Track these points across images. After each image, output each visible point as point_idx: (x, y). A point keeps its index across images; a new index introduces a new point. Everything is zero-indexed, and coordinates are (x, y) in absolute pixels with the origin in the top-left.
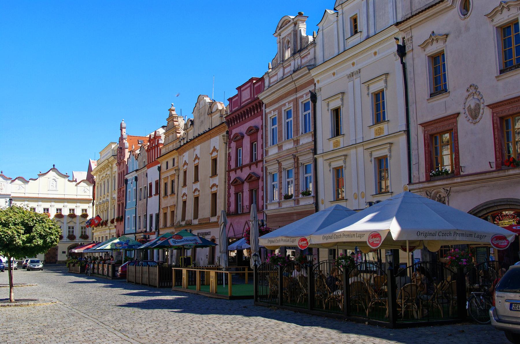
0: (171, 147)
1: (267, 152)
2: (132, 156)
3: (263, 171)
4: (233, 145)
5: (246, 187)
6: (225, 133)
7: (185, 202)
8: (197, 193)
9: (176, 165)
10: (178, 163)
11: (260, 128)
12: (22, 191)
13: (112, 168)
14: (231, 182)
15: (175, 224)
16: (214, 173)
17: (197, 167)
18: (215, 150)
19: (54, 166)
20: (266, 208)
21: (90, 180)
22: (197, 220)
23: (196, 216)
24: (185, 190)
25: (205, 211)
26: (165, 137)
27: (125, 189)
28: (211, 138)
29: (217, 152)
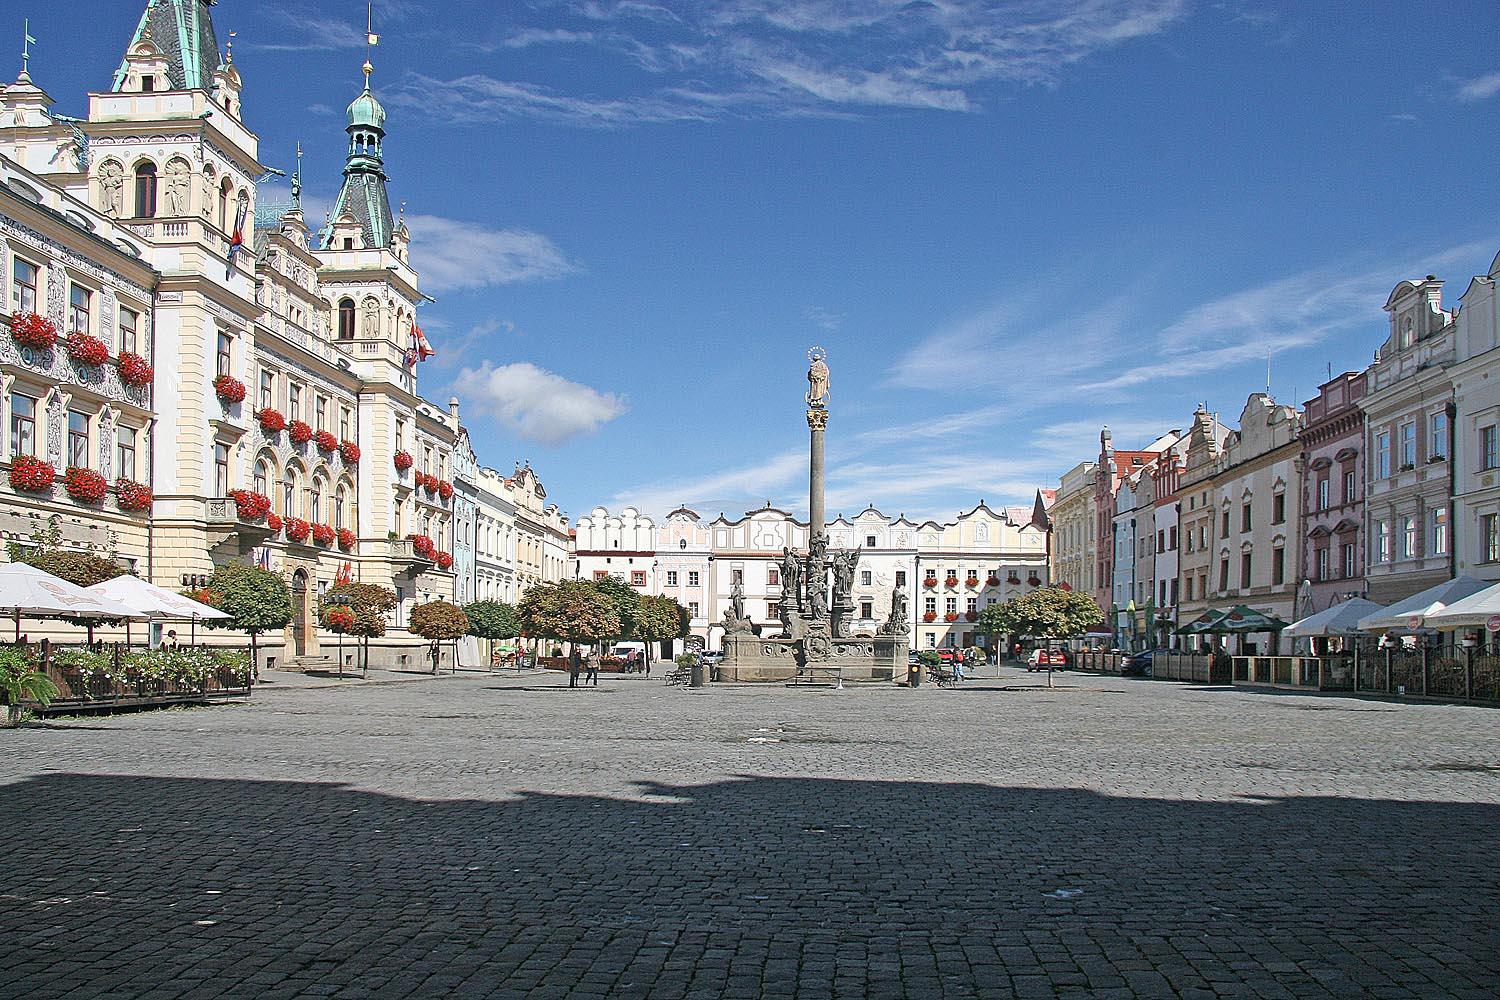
0: (1199, 474)
1: (1371, 488)
2: (1124, 485)
3: (1363, 517)
4: (1313, 475)
5: (1335, 541)
6: (1298, 457)
7: (1225, 563)
8: (1247, 549)
9: (1208, 503)
10: (1212, 499)
11: (1360, 451)
12: (935, 543)
13: (1085, 504)
14: (1308, 533)
15: (1208, 596)
16: (1279, 518)
17: (1247, 508)
18: (1280, 481)
19: (982, 501)
20: (1369, 573)
21: (1040, 519)
22: (1249, 590)
23: (1246, 583)
24: (1226, 543)
25: (1262, 575)
26: (1188, 458)
27: (1112, 539)
28: (1273, 463)
29: (1285, 485)
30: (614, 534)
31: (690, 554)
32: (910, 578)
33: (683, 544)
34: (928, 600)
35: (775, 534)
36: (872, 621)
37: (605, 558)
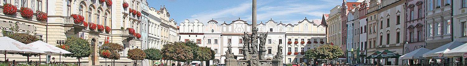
0: (373, 9)
1: (427, 14)
2: (350, 13)
3: (424, 23)
4: (409, 10)
5: (416, 30)
6: (404, 4)
7: (381, 37)
8: (388, 32)
9: (376, 18)
10: (377, 17)
11: (423, 2)
12: (291, 30)
13: (338, 19)
14: (407, 27)
15: (376, 47)
16: (398, 23)
17: (388, 20)
18: (398, 11)
19: (306, 18)
20: (426, 40)
21: (324, 23)
23: (388, 43)
24: (382, 31)
25: (393, 41)
26: (370, 4)
27: (346, 29)
28: (396, 6)
29: (400, 13)
30: (191, 28)
31: (215, 34)
32: (283, 41)
33: (213, 31)
34: (289, 48)
35: (241, 28)
36: (272, 55)
37: (188, 35)
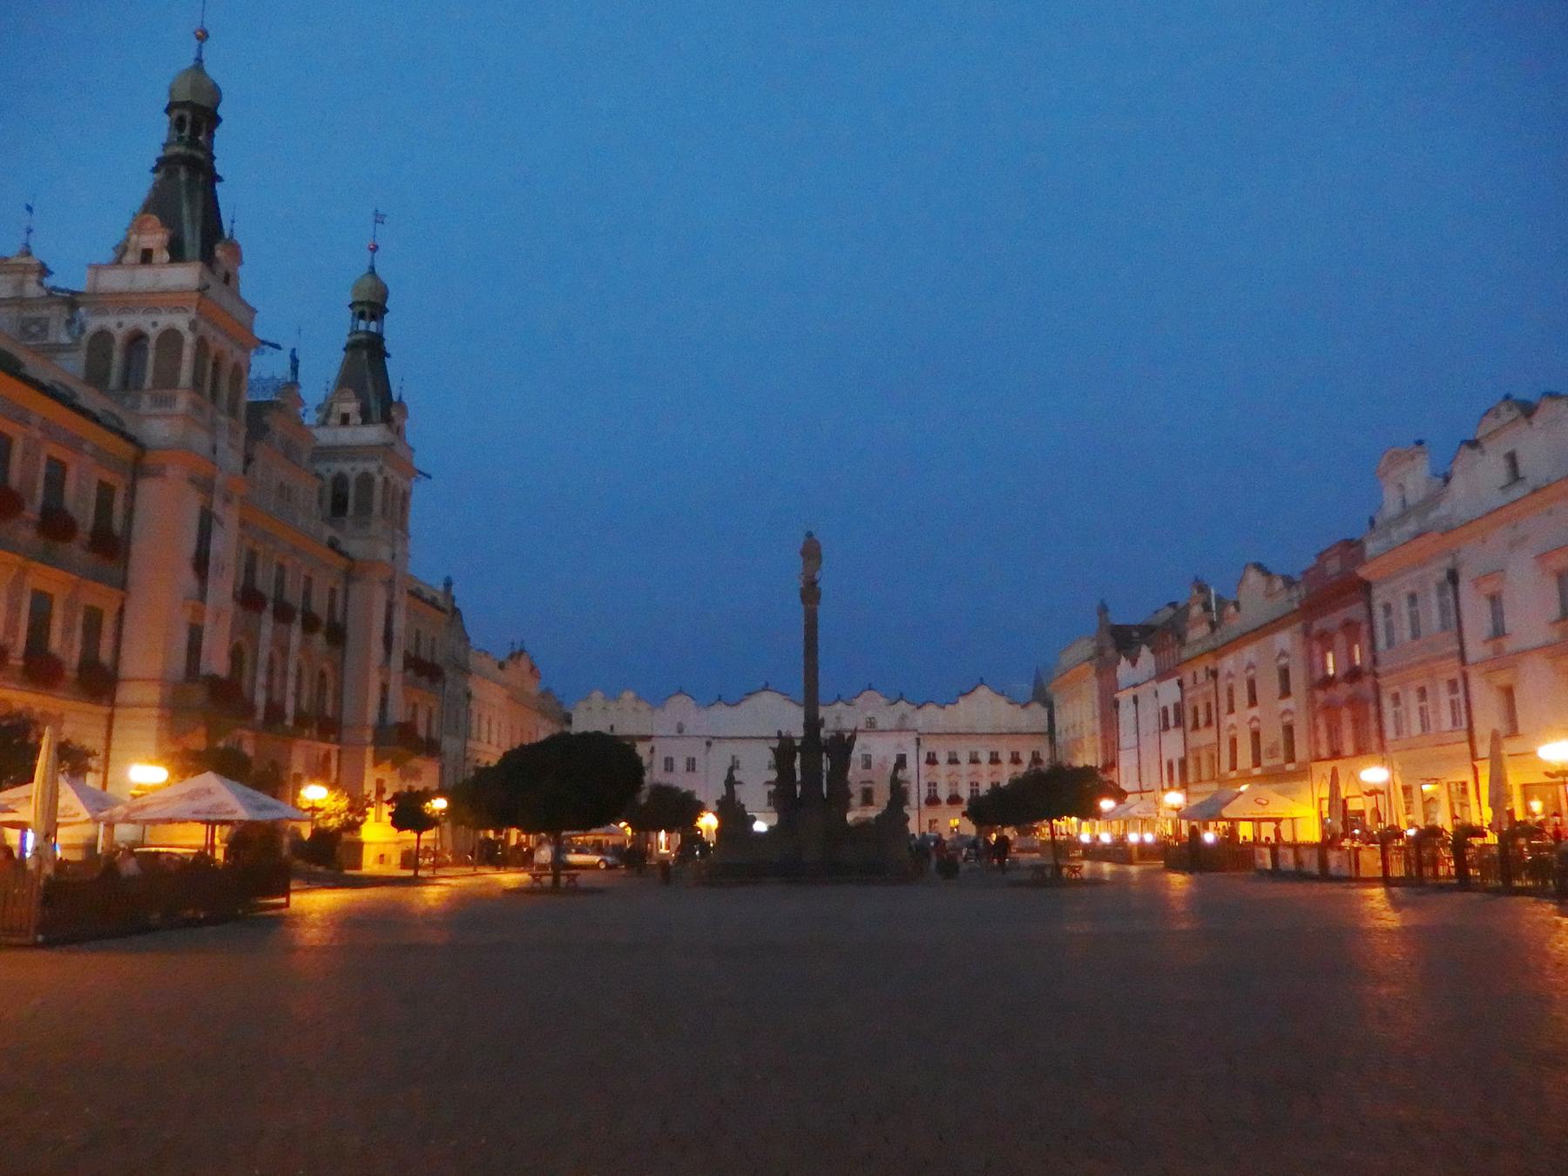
16: (1286, 692)
24: (1232, 719)
33: (680, 730)
